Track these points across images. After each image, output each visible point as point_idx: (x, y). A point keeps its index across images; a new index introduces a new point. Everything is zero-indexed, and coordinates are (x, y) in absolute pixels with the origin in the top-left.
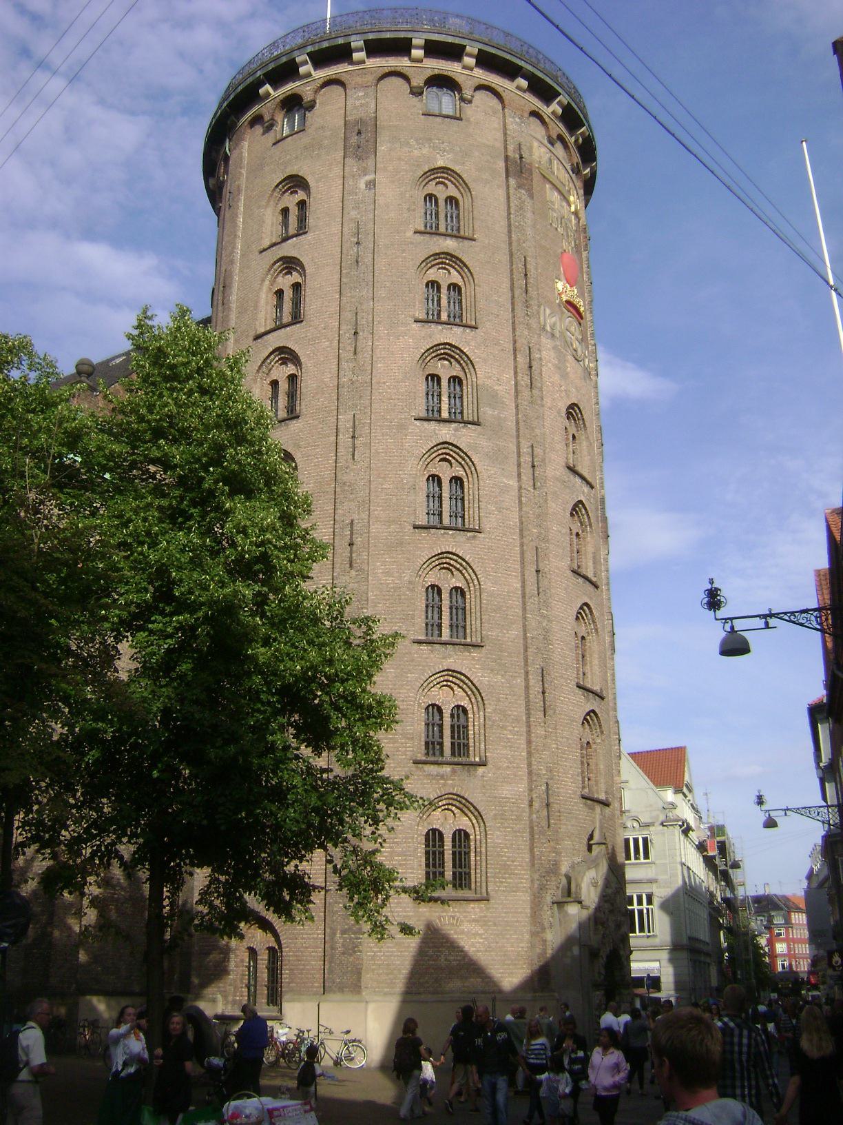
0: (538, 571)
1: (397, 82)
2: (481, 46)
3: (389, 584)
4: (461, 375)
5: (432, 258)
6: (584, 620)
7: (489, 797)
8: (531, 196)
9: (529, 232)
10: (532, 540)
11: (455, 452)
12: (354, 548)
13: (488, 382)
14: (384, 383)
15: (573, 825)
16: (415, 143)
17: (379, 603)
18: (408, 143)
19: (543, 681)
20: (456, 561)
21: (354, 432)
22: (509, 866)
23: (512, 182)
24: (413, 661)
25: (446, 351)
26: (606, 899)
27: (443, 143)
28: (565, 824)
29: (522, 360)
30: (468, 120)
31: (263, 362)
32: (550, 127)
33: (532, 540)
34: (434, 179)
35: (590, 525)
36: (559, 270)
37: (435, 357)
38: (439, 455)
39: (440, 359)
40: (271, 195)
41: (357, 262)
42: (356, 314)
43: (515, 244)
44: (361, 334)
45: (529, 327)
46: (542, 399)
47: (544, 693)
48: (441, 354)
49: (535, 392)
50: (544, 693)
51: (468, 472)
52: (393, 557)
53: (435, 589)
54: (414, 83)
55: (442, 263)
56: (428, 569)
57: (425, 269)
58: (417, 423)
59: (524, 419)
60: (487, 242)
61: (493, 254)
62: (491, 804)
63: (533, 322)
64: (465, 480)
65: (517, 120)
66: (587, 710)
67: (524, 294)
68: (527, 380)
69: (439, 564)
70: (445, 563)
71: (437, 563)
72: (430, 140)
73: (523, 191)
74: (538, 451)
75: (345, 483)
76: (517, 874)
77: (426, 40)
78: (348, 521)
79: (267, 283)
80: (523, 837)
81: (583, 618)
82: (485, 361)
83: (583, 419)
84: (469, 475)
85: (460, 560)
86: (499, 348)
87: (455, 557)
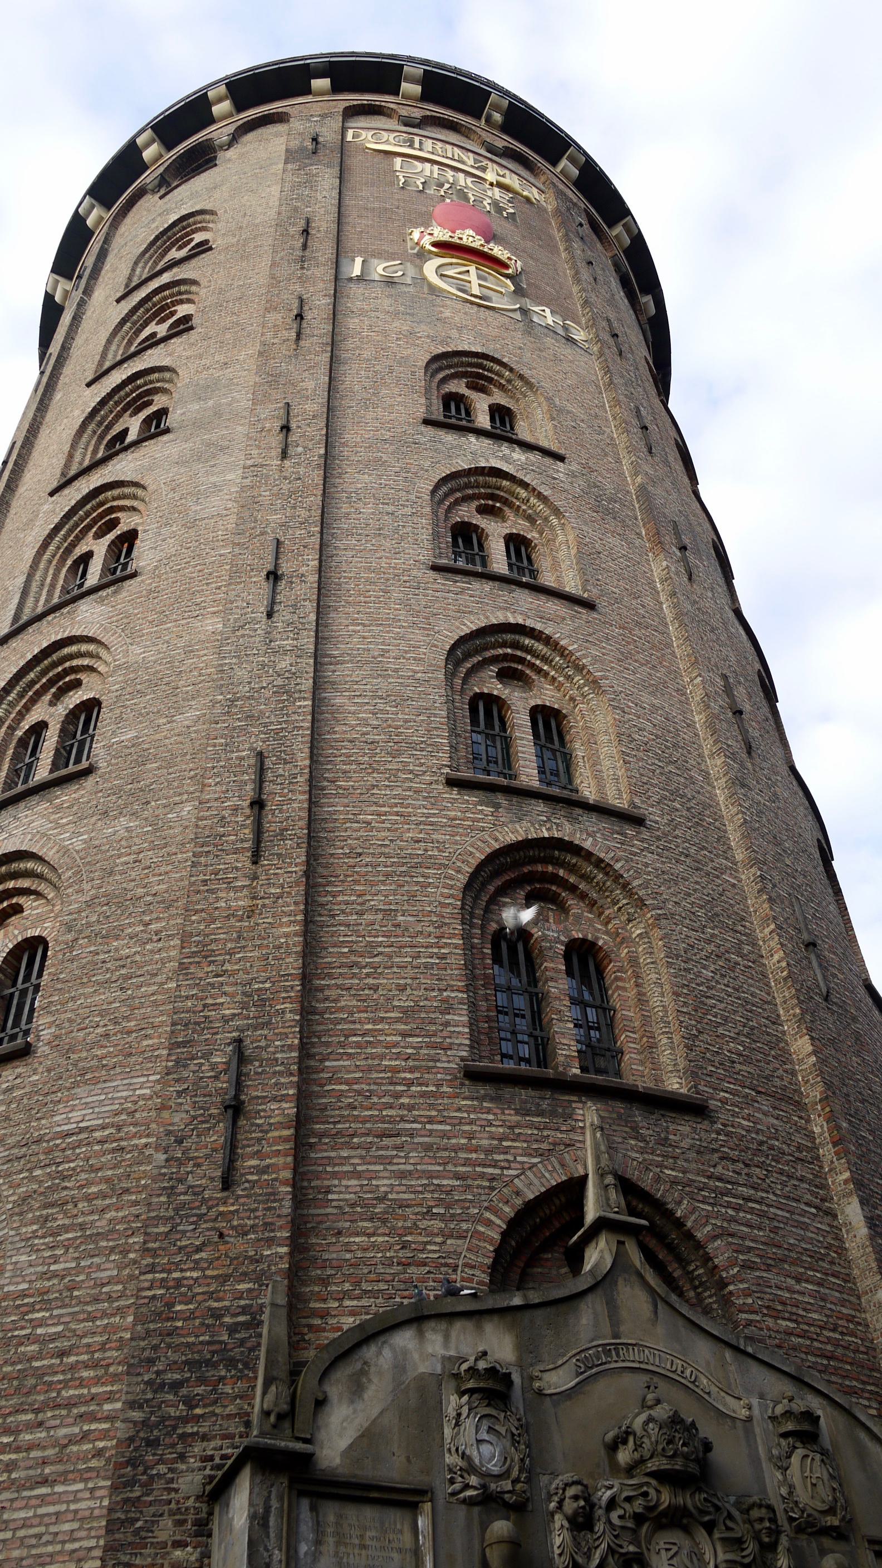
6: (539, 671)
7: (19, 1145)
15: (402, 1175)
22: (40, 1374)
26: (624, 1456)
28: (357, 1175)
35: (557, 512)
38: (95, 521)
47: (258, 804)
50: (258, 804)
55: (162, 309)
62: (17, 1166)
69: (52, 682)
70: (66, 672)
76: (69, 1405)
80: (124, 1253)
83: (521, 377)
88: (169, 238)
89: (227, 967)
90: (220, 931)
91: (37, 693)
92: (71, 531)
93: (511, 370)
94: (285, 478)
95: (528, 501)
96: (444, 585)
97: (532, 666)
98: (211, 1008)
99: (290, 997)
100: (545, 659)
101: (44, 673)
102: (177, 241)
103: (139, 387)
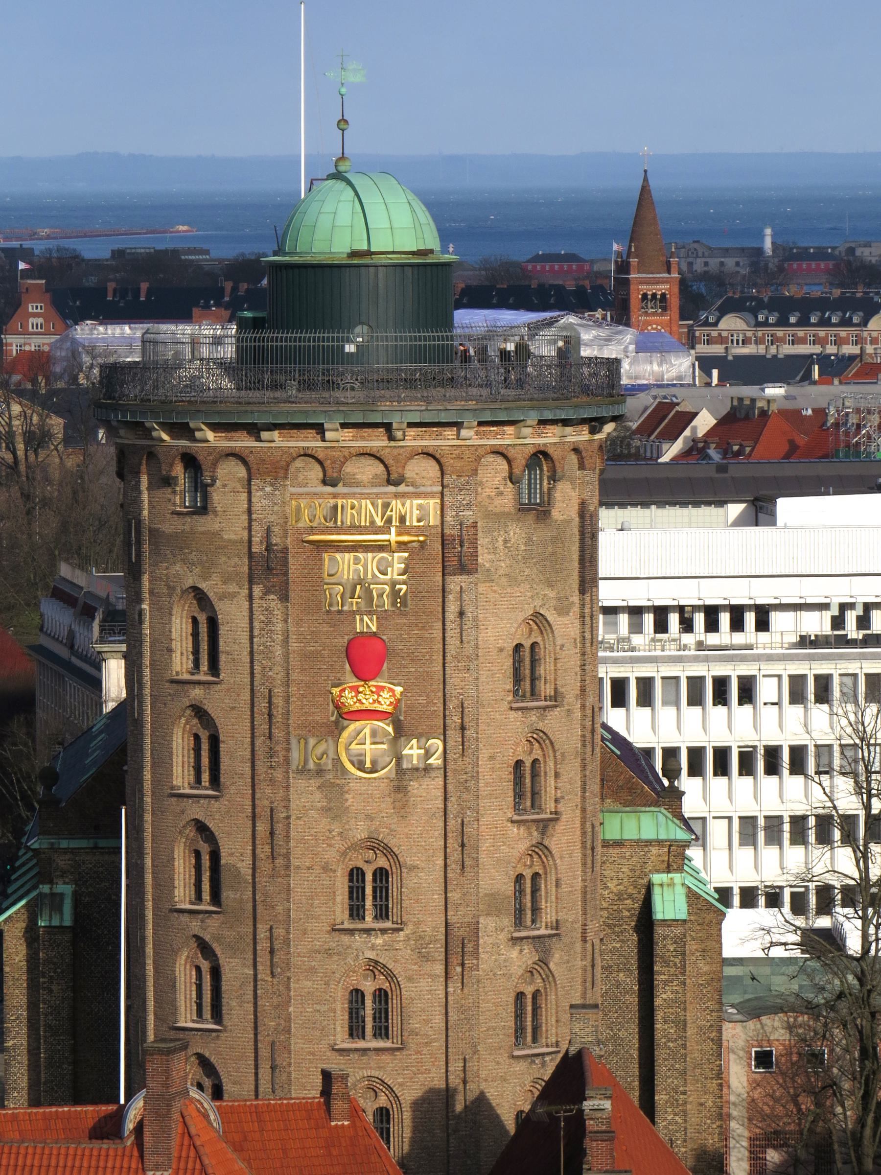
8: (285, 598)
10: (268, 1035)
23: (257, 591)
29: (262, 827)
30: (215, 513)
33: (268, 1035)
36: (343, 668)
43: (258, 677)
49: (280, 861)
60: (232, 681)
61: (238, 695)
65: (268, 489)
67: (268, 742)
72: (182, 548)
73: (272, 597)
74: (280, 932)
86: (244, 815)
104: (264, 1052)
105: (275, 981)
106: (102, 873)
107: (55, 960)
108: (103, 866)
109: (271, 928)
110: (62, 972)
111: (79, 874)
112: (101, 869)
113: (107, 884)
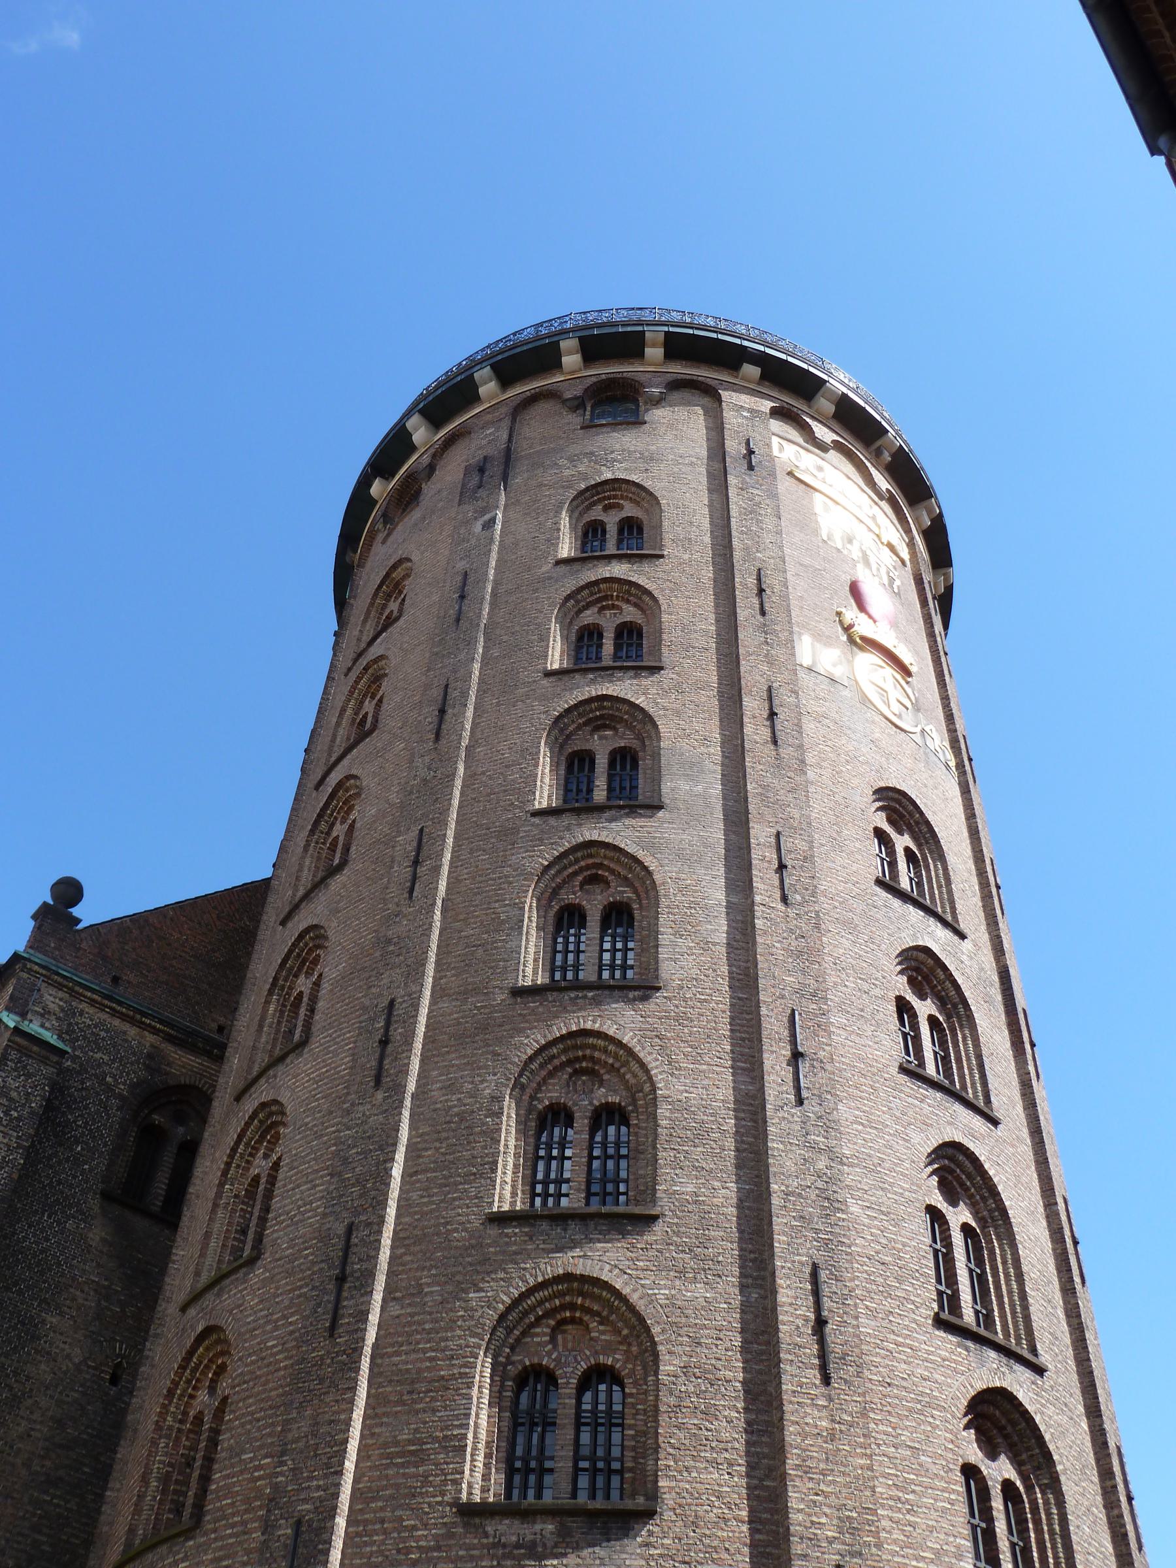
0: (796, 1056)
1: (543, 407)
2: (666, 329)
3: (450, 1107)
4: (635, 744)
5: (586, 592)
9: (768, 538)
11: (611, 859)
12: (390, 1048)
13: (684, 744)
14: (483, 773)
16: (566, 462)
17: (426, 1149)
18: (556, 464)
19: (816, 1293)
20: (605, 1051)
21: (418, 855)
24: (482, 1263)
25: (605, 712)
27: (612, 452)
31: (320, 816)
32: (815, 429)
33: (783, 997)
34: (600, 500)
37: (585, 724)
38: (581, 870)
39: (597, 729)
40: (372, 604)
41: (458, 620)
42: (447, 686)
43: (737, 555)
44: (450, 711)
45: (770, 661)
46: (803, 761)
48: (597, 718)
49: (786, 752)
51: (640, 889)
52: (464, 1056)
53: (559, 1115)
54: (568, 395)
55: (606, 598)
56: (544, 1073)
57: (576, 609)
58: (537, 820)
59: (760, 790)
60: (686, 557)
63: (779, 653)
64: (635, 906)
66: (980, 1386)
67: (759, 617)
68: (766, 733)
69: (569, 1062)
71: (564, 1058)
72: (592, 453)
75: (389, 941)
77: (580, 338)
78: (386, 1003)
79: (349, 712)
81: (958, 1179)
82: (678, 713)
84: (643, 895)
85: (611, 1048)
87: (601, 1043)
88: (598, 493)
89: (823, 1487)
90: (812, 1449)
91: (556, 1069)
92: (559, 872)
93: (921, 813)
94: (791, 931)
95: (944, 983)
96: (912, 1088)
97: (962, 1184)
98: (817, 1526)
99: (871, 1531)
100: (969, 1177)
101: (565, 1051)
102: (605, 498)
103: (604, 708)
104: (773, 1025)
105: (791, 912)
106: (103, 1039)
107: (14, 1094)
108: (107, 1031)
109: (778, 835)
110: (19, 1119)
111: (70, 1024)
112: (103, 1034)
113: (106, 1058)
